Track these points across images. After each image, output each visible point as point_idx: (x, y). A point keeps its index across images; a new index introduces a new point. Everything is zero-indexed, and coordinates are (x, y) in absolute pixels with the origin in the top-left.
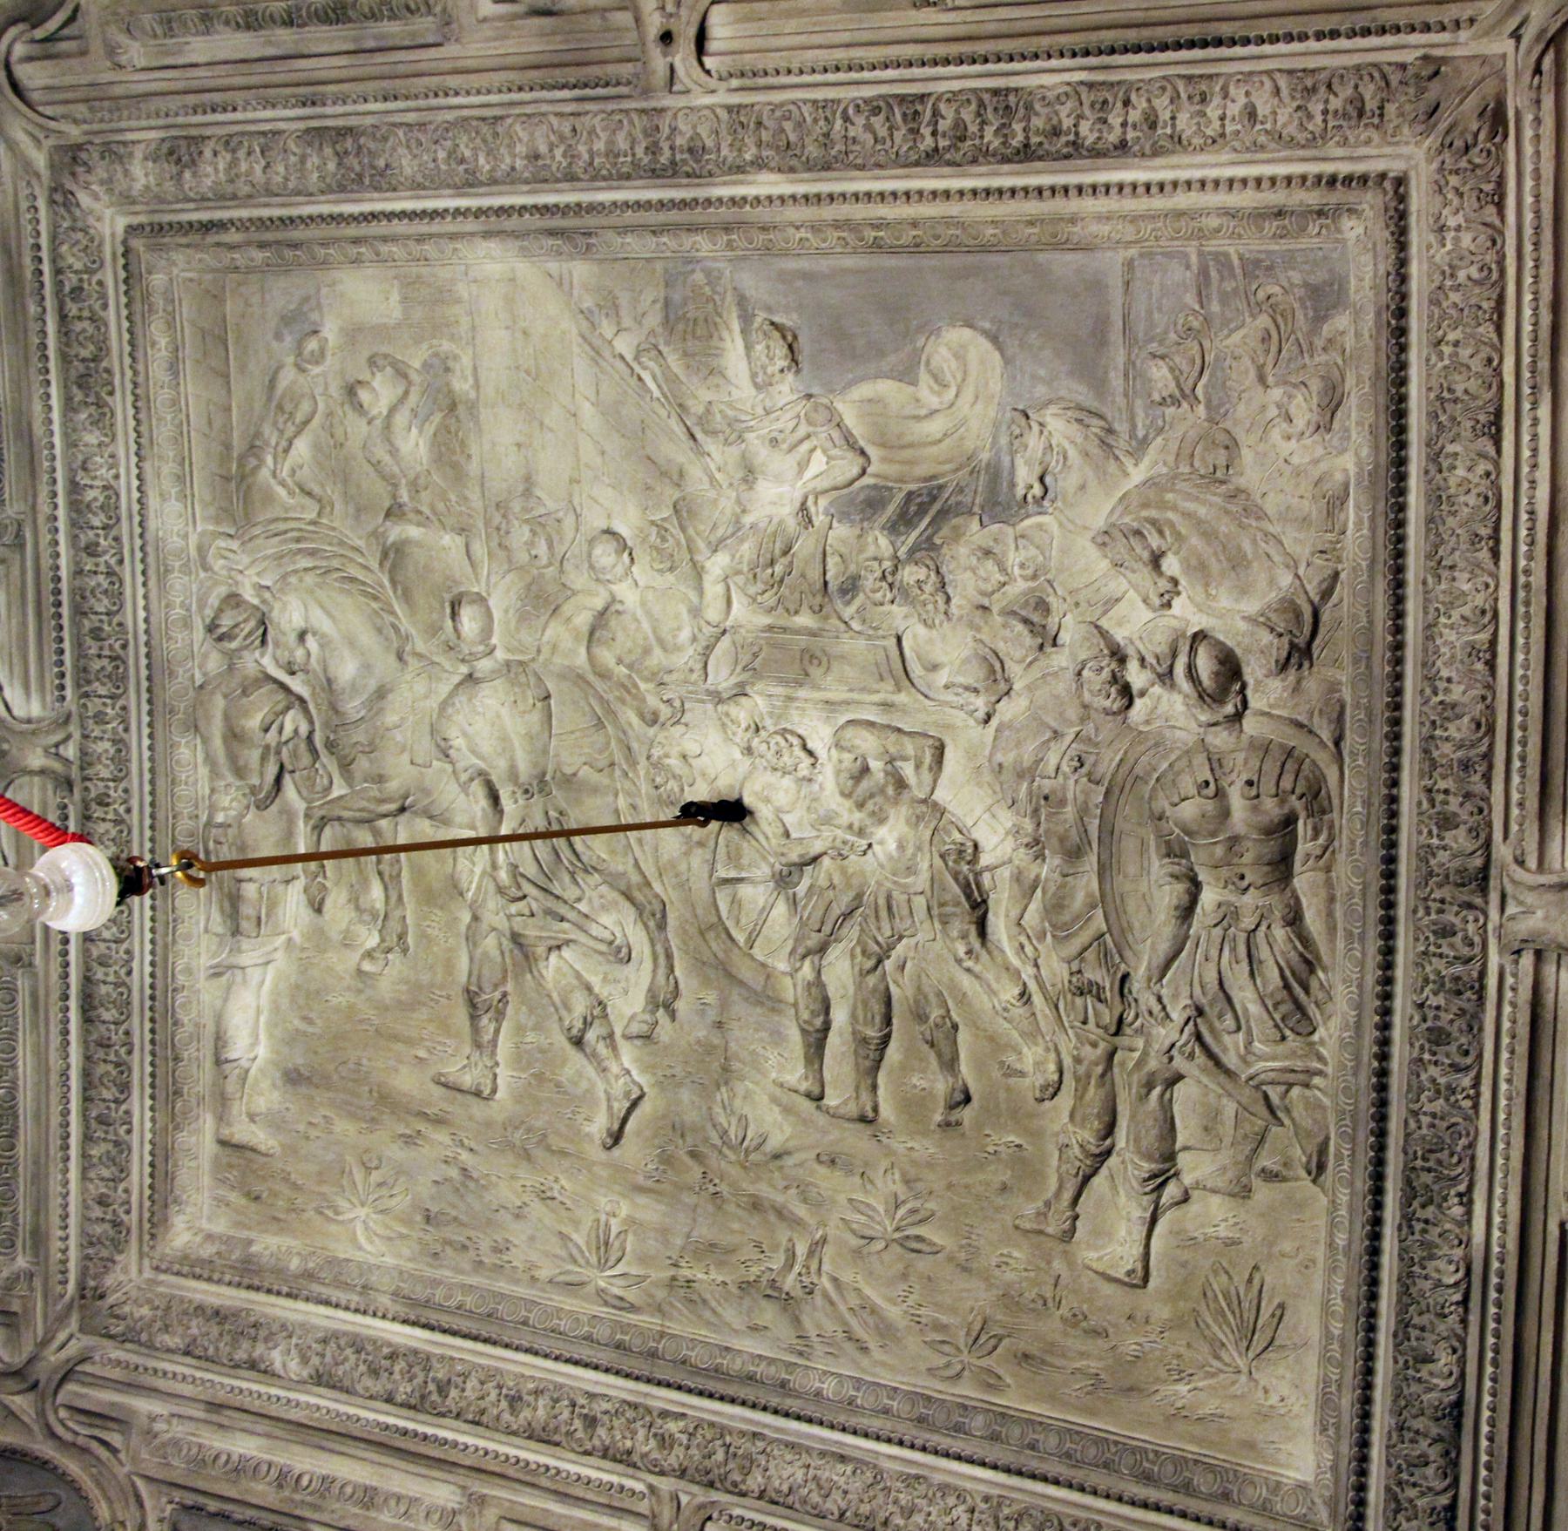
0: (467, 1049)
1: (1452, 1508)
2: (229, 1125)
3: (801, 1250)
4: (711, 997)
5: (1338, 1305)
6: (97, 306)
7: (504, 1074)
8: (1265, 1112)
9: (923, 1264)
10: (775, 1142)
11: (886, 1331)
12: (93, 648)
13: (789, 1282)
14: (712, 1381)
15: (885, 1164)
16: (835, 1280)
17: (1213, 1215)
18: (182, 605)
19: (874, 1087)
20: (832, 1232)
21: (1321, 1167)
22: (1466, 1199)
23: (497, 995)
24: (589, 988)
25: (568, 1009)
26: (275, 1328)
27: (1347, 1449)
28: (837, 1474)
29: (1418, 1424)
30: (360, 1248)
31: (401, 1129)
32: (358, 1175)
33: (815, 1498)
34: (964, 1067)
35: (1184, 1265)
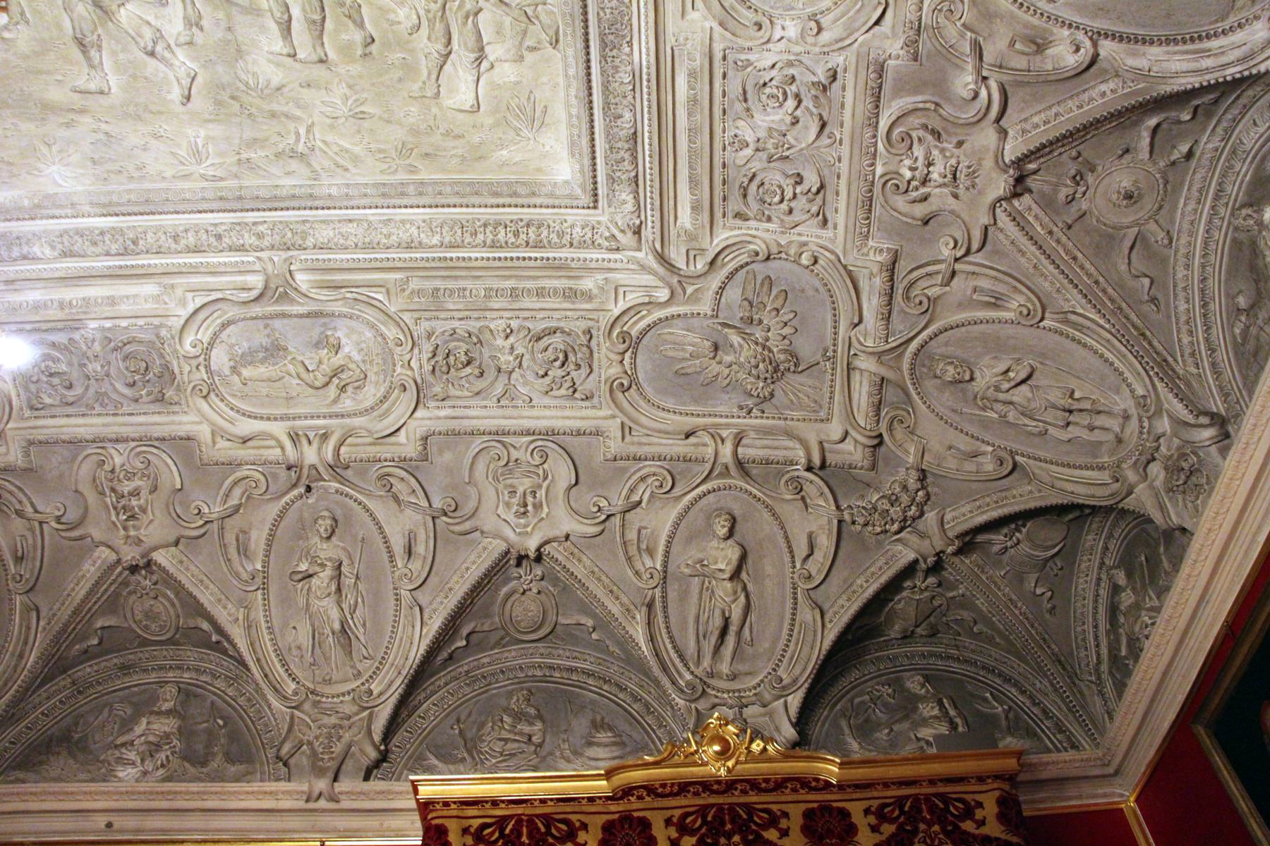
0: (87, 71)
1: (637, 176)
3: (302, 131)
4: (221, 15)
5: (574, 101)
7: (113, 80)
8: (526, 20)
9: (366, 124)
10: (276, 81)
11: (356, 159)
13: (301, 148)
14: (275, 203)
15: (336, 80)
16: (324, 141)
17: (507, 73)
19: (323, 44)
20: (316, 119)
21: (557, 41)
22: (630, 44)
23: (95, 37)
24: (148, 23)
25: (141, 37)
26: (30, 236)
27: (587, 162)
28: (351, 229)
29: (619, 145)
30: (61, 186)
31: (62, 120)
32: (45, 150)
33: (342, 241)
34: (367, 25)
35: (496, 97)
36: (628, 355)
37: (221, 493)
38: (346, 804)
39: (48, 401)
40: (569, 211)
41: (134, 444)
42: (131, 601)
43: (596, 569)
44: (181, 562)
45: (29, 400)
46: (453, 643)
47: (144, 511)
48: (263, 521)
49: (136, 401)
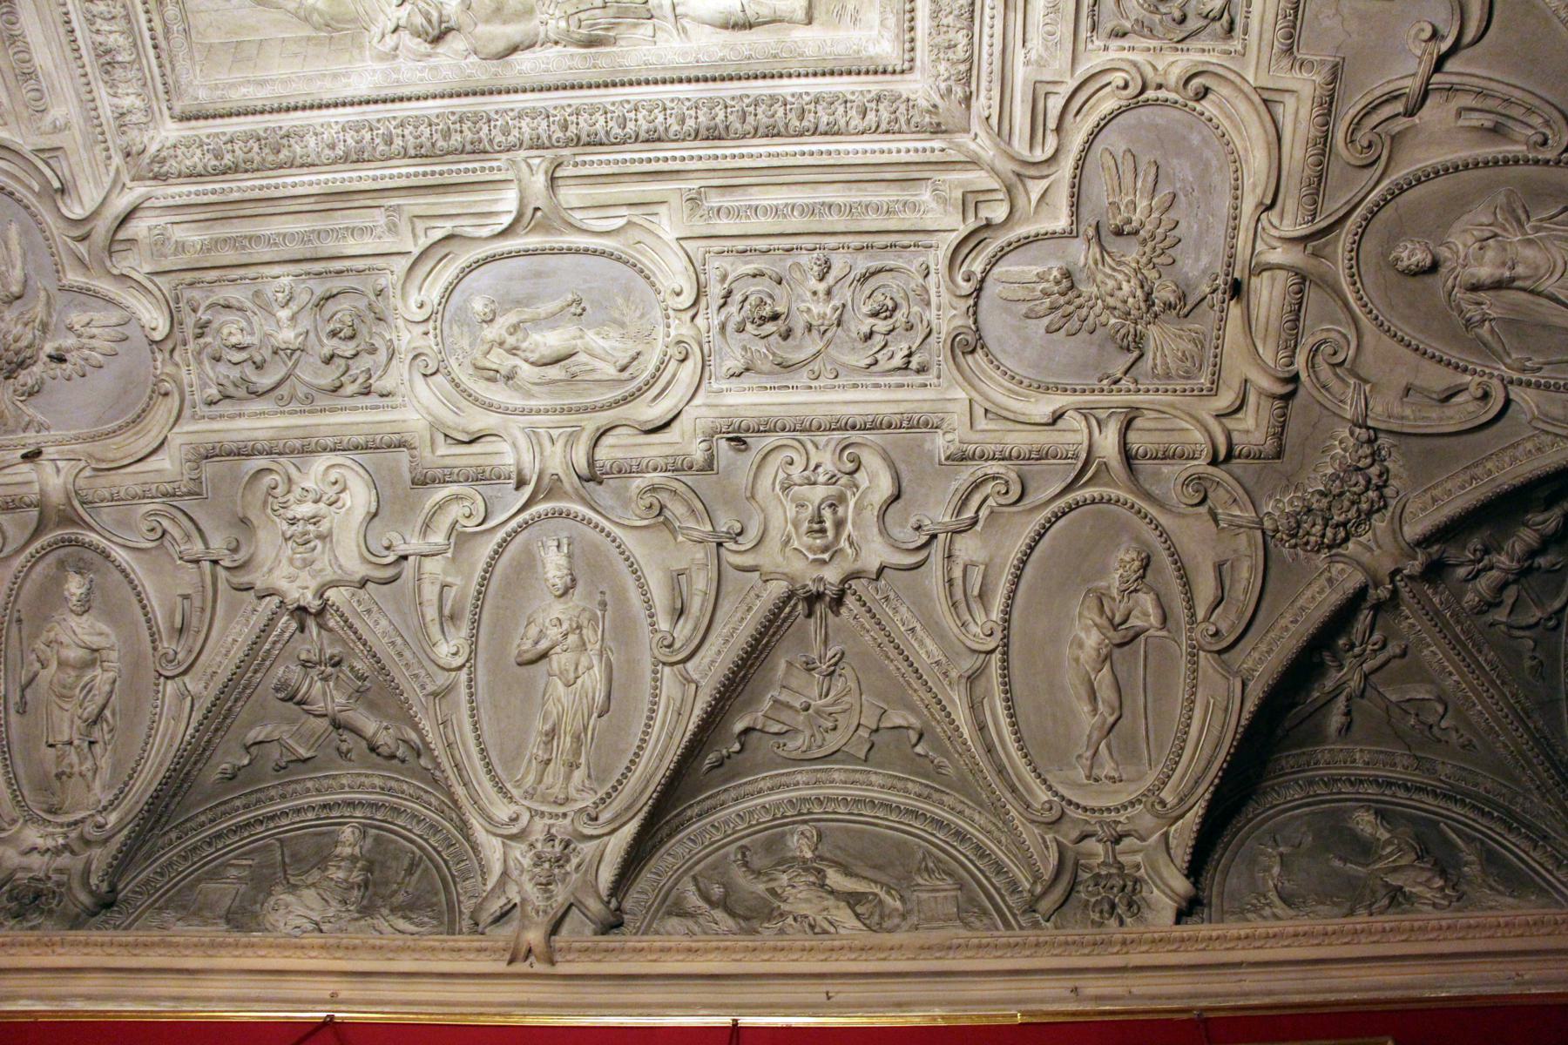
2: (794, 11)
6: (224, 139)
12: (456, 140)
18: (421, 71)
45: (1215, 37)
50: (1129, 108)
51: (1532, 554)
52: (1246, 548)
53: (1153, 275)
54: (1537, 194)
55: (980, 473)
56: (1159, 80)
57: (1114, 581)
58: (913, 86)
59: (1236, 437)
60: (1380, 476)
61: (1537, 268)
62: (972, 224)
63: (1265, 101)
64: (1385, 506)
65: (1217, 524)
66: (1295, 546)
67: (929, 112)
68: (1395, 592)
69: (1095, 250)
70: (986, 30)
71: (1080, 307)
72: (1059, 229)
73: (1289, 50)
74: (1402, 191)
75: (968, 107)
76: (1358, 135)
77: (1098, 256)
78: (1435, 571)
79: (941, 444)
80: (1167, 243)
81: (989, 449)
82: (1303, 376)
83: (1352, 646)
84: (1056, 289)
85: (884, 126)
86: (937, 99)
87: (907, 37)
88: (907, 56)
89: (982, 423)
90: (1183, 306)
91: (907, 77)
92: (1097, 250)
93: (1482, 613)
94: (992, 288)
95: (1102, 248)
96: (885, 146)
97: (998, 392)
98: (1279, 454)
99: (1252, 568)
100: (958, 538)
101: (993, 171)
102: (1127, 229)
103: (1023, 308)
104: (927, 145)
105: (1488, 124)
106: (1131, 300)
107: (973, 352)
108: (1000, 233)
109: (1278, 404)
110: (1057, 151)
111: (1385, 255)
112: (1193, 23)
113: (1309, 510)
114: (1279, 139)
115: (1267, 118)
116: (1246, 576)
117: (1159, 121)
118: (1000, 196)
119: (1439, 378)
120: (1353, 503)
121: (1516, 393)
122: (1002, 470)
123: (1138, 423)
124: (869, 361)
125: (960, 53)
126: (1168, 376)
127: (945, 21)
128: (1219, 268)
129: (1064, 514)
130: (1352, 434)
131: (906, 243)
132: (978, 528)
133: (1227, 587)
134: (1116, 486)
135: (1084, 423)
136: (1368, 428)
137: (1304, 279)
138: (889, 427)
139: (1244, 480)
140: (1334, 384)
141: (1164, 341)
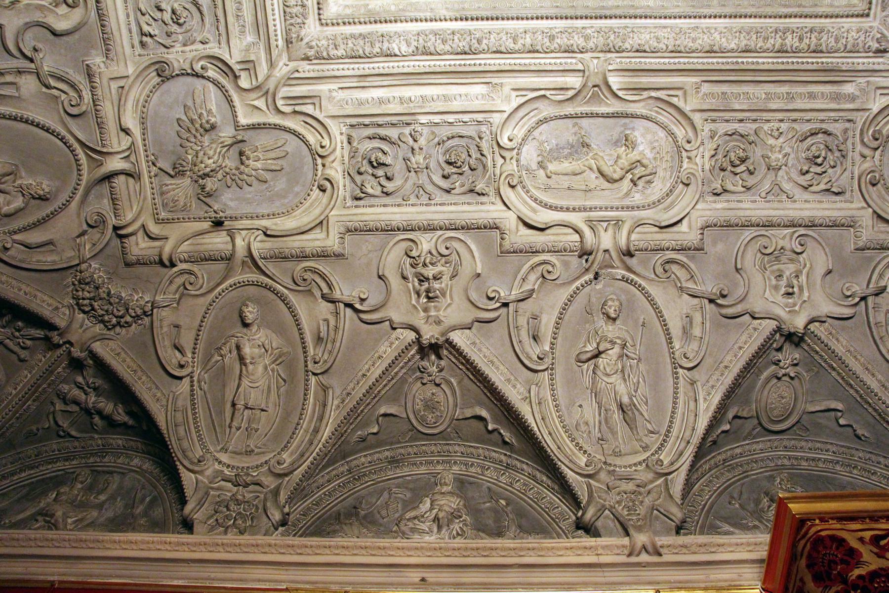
36: (878, 152)
37: (519, 277)
38: (667, 558)
39: (370, 191)
40: (844, 20)
41: (440, 233)
42: (415, 388)
43: (852, 349)
44: (474, 343)
45: (352, 191)
46: (719, 427)
47: (444, 295)
48: (552, 307)
49: (448, 192)
50: (310, 150)
51: (100, 413)
52: (66, 256)
53: (220, 176)
54: (290, 366)
55: (81, 87)
56: (327, 164)
57: (27, 180)
58: (312, 26)
59: (133, 238)
60: (126, 323)
61: (253, 375)
62: (236, 67)
63: (321, 222)
64: (109, 329)
65: (78, 236)
66: (74, 284)
67: (298, 36)
68: (59, 346)
69: (229, 141)
70: (346, 66)
71: (195, 137)
72: (239, 119)
73: (349, 231)
74: (283, 301)
75: (303, 59)
76: (309, 273)
77: (226, 143)
78: (77, 365)
79: (97, 60)
80: (239, 182)
81: (99, 92)
82: (175, 269)
83: (19, 331)
84: (204, 121)
85: (288, 10)
86: (305, 41)
87: (340, 21)
88: (329, 21)
89: (114, 85)
90: (205, 196)
91: (317, 22)
92: (229, 142)
93: (58, 396)
94: (198, 83)
95: (231, 145)
96: (276, 12)
97: (136, 93)
98: (128, 265)
99: (54, 262)
100: (34, 77)
101: (268, 77)
102: (244, 158)
103: (190, 103)
104: (279, 37)
105: (322, 335)
106: (203, 165)
107: (159, 75)
108: (233, 85)
109: (157, 259)
110: (283, 113)
111: (249, 299)
112: (358, 179)
113: (97, 288)
114: (303, 233)
115: (313, 225)
116: (48, 259)
117: (306, 167)
118: (254, 83)
119: (187, 341)
120: (107, 311)
121: (187, 380)
122: (86, 101)
123: (131, 180)
124: (143, 9)
125: (333, 52)
126: (162, 194)
127: (350, 42)
128: (229, 213)
129: (65, 143)
130: (147, 302)
131: (220, 28)
132: (44, 90)
133: (38, 250)
134: (89, 173)
135: (125, 148)
136: (152, 310)
137: (229, 260)
138: (102, 26)
139: (108, 248)
140: (174, 287)
141: (182, 189)
